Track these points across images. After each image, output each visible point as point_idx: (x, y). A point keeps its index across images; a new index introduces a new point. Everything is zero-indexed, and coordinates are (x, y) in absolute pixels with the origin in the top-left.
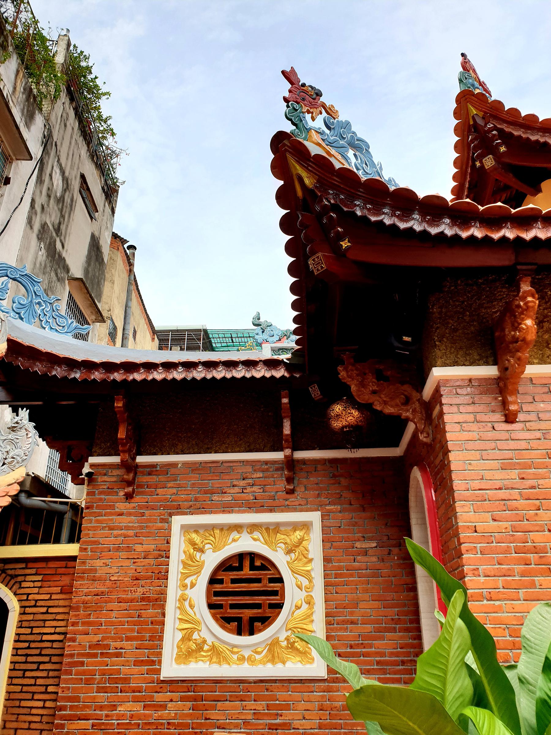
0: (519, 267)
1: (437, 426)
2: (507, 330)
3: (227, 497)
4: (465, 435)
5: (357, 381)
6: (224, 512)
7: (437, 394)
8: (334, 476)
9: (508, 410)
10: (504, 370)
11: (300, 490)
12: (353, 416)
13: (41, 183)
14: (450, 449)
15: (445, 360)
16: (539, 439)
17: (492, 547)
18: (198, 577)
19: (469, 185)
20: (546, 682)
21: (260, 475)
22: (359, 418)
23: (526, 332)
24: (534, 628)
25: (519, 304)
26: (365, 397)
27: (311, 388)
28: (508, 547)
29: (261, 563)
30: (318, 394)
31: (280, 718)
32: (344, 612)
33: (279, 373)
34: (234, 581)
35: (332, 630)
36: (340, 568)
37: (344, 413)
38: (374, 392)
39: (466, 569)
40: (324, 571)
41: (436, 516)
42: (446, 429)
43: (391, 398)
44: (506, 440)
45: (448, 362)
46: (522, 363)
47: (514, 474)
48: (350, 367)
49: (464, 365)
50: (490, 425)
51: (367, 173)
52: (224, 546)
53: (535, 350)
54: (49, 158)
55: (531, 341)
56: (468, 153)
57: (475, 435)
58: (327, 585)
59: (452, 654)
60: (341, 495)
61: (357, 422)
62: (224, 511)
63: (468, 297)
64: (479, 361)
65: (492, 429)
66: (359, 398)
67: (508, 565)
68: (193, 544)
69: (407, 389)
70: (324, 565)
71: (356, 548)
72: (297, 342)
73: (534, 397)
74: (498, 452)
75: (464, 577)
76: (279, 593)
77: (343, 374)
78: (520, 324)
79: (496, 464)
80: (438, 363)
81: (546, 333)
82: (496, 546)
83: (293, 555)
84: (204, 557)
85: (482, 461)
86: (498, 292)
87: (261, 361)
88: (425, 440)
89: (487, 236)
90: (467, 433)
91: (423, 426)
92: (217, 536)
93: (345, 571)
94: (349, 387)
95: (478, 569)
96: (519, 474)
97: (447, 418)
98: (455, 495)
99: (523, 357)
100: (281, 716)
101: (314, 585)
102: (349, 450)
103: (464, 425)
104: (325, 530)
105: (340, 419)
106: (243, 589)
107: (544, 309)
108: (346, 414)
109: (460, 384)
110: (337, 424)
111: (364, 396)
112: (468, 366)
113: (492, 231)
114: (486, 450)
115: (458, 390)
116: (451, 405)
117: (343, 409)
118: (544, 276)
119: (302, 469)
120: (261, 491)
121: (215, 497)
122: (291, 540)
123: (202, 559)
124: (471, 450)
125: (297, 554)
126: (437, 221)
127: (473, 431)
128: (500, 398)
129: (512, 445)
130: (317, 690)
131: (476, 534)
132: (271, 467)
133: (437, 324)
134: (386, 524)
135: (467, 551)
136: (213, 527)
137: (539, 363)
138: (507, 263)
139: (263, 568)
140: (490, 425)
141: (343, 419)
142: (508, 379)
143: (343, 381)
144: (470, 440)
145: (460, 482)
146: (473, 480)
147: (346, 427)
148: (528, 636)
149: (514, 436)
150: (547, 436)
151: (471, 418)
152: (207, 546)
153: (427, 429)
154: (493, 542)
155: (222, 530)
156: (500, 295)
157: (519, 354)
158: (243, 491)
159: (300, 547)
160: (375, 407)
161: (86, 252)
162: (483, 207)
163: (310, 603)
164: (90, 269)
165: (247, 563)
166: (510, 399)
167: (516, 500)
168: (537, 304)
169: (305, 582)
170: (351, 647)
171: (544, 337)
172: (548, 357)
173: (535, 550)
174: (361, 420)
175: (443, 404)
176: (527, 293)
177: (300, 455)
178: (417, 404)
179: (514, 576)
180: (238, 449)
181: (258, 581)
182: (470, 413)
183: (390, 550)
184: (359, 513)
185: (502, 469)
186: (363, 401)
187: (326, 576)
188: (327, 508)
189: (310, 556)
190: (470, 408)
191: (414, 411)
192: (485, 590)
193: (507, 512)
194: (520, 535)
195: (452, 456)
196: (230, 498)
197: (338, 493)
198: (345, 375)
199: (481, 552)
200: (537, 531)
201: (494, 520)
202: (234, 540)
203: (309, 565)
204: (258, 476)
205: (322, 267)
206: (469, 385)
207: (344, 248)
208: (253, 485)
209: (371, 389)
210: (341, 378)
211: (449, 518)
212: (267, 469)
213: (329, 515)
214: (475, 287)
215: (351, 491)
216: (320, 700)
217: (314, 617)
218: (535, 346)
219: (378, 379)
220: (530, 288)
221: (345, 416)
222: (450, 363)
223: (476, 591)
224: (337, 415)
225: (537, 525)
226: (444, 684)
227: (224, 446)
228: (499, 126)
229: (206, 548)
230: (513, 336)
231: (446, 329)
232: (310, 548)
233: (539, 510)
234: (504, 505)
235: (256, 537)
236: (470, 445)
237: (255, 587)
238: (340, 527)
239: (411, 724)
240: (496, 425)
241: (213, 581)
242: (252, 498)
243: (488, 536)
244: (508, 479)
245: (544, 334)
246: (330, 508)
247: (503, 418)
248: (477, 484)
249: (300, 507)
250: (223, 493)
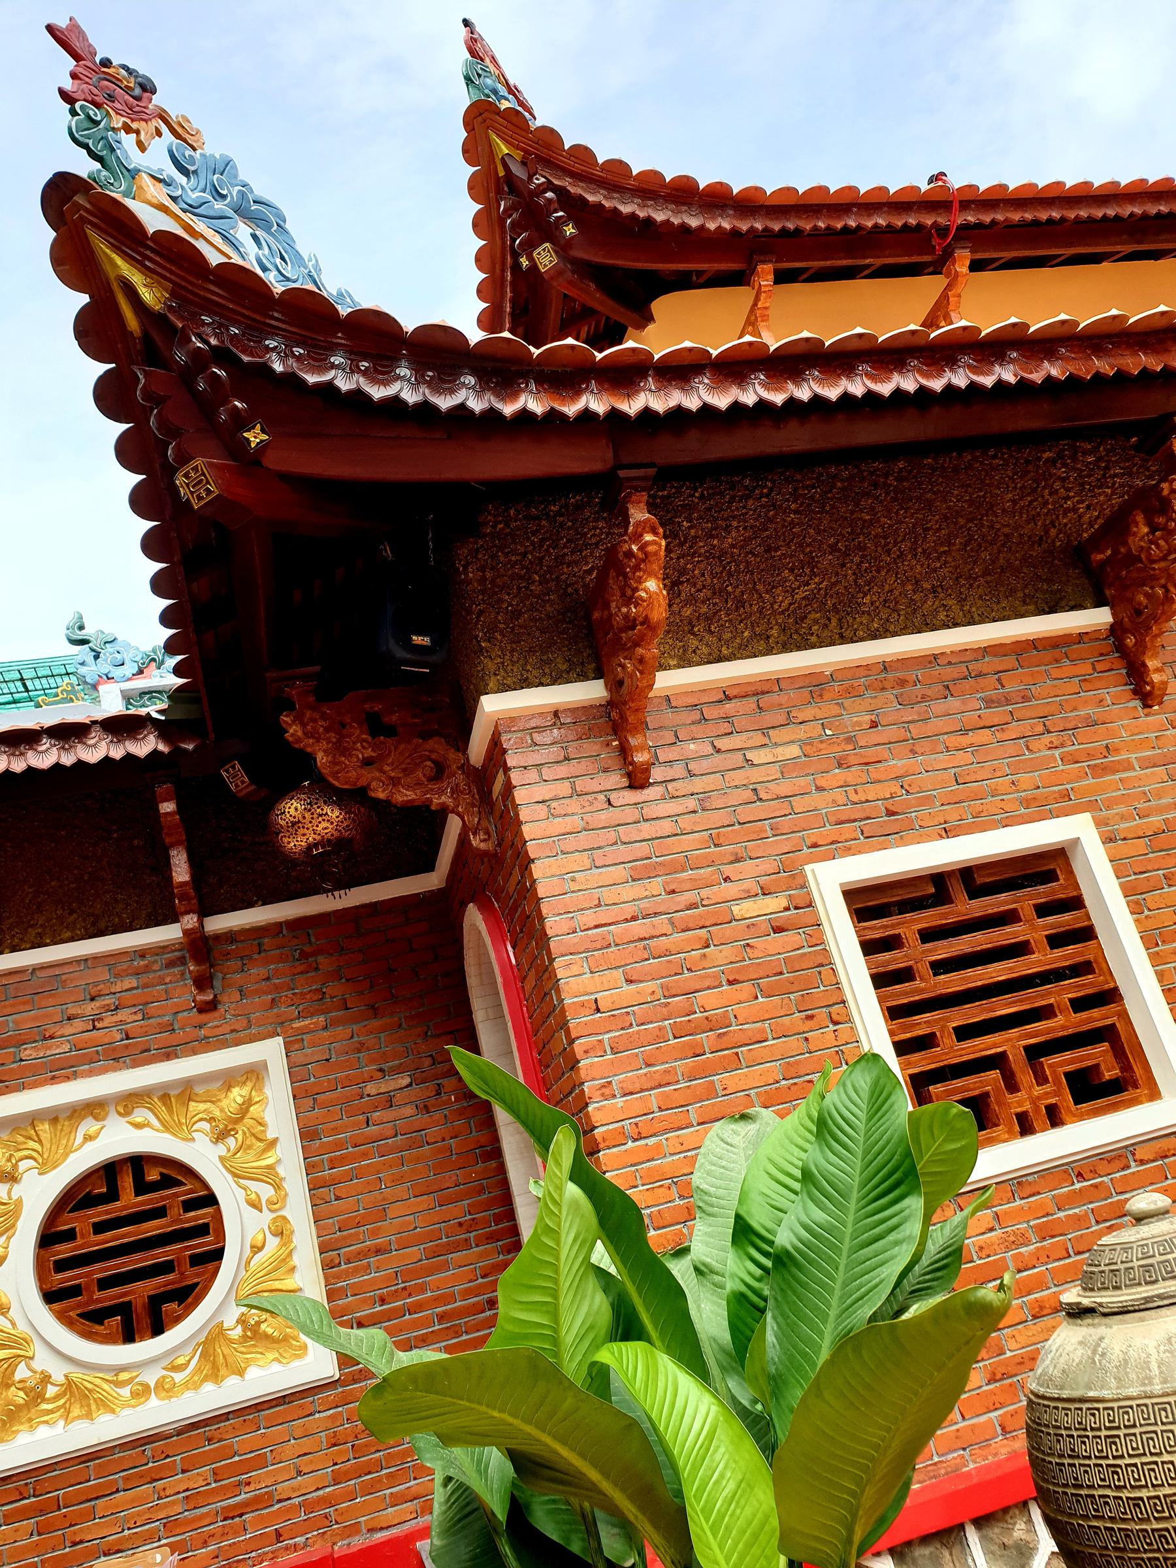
0: (622, 474)
1: (504, 815)
2: (613, 605)
3: (58, 1047)
4: (559, 825)
5: (327, 744)
6: (54, 1080)
7: (496, 750)
8: (304, 955)
9: (632, 763)
10: (615, 685)
11: (230, 1001)
12: (328, 821)
14: (532, 856)
15: (504, 678)
16: (694, 812)
17: (630, 1035)
18: (9, 1238)
19: (513, 307)
20: (740, 1258)
21: (131, 982)
22: (342, 822)
23: (648, 605)
24: (713, 1168)
25: (631, 549)
26: (350, 774)
27: (227, 771)
28: (660, 1029)
29: (161, 1174)
30: (243, 782)
31: (247, 1489)
32: (358, 1234)
33: (145, 746)
34: (99, 1228)
35: (338, 1277)
36: (339, 1145)
37: (308, 815)
38: (367, 762)
39: (589, 1088)
40: (305, 1159)
41: (522, 996)
42: (521, 818)
43: (404, 770)
44: (635, 823)
45: (509, 681)
46: (649, 669)
47: (656, 885)
48: (308, 714)
49: (541, 684)
50: (601, 797)
51: (288, 279)
52: (66, 1155)
53: (671, 642)
55: (658, 623)
56: (503, 239)
57: (576, 822)
58: (314, 1186)
59: (563, 1257)
60: (324, 993)
61: (340, 831)
62: (53, 1078)
63: (533, 543)
64: (568, 673)
65: (606, 806)
66: (337, 779)
67: (663, 1063)
69: (437, 746)
70: (303, 1147)
71: (369, 1095)
72: (178, 671)
73: (676, 732)
74: (622, 847)
75: (587, 1105)
76: (214, 1228)
77: (294, 731)
78: (636, 590)
79: (620, 872)
80: (491, 685)
81: (686, 605)
82: (638, 1032)
83: (231, 1141)
84: (17, 1190)
85: (595, 871)
86: (590, 530)
87: (94, 722)
88: (483, 846)
89: (552, 409)
90: (560, 819)
91: (476, 819)
92: (45, 1136)
93: (351, 1149)
94: (311, 758)
95: (610, 1083)
96: (665, 884)
97: (520, 795)
98: (552, 944)
99: (648, 655)
100: (249, 1484)
101: (286, 1195)
102: (330, 894)
103: (554, 804)
104: (296, 1072)
105: (301, 831)
106: (126, 1240)
107: (678, 558)
108: (312, 818)
109: (538, 724)
110: (295, 843)
111: (348, 772)
112: (548, 685)
113: (563, 401)
114: (599, 848)
115: (535, 735)
116: (525, 768)
117: (305, 809)
118: (673, 491)
119: (228, 954)
120: (140, 1016)
121: (28, 1052)
122: (222, 1110)
123: (15, 1197)
124: (572, 853)
125: (240, 1136)
126: (449, 382)
127: (573, 814)
128: (615, 743)
129: (647, 829)
130: (321, 1408)
131: (599, 1015)
132: (156, 961)
133: (479, 605)
134: (426, 1033)
135: (586, 1052)
136: (32, 1119)
137: (679, 666)
138: (597, 466)
139: (167, 1182)
140: (601, 797)
141: (308, 829)
142: (625, 703)
143: (297, 746)
144: (568, 833)
145: (557, 918)
146: (582, 910)
147: (316, 845)
148: (704, 1186)
149: (649, 812)
150: (707, 805)
151: (564, 788)
152: (23, 1165)
153: (484, 823)
154: (631, 1024)
155: (55, 1120)
156: (594, 535)
157: (640, 651)
158: (94, 1027)
159: (246, 1121)
160: (373, 795)
162: (538, 348)
163: (282, 1233)
165: (127, 1182)
166: (633, 741)
167: (665, 935)
168: (663, 548)
169: (266, 1192)
170: (383, 1301)
171: (683, 613)
172: (694, 652)
173: (710, 1024)
174: (347, 826)
175: (510, 769)
176: (644, 526)
177: (219, 923)
178: (460, 778)
179: (677, 1082)
180: (69, 934)
181: (160, 1213)
182: (563, 779)
183: (438, 1085)
184: (366, 1023)
185: (634, 880)
186: (346, 783)
187: (310, 1169)
188: (296, 1025)
189: (270, 1135)
190: (563, 770)
191: (455, 791)
192: (628, 1122)
193: (651, 961)
194: (680, 1002)
195: (537, 870)
196: (66, 1047)
198: (300, 733)
199: (612, 1048)
200: (709, 988)
201: (630, 981)
202: (88, 1138)
203: (270, 1154)
204: (127, 985)
205: (209, 492)
206: (555, 724)
207: (253, 445)
208: (117, 1008)
209: (360, 756)
210: (290, 739)
211: (545, 994)
212: (147, 966)
213: (303, 1040)
214: (544, 522)
215: (344, 980)
216: (330, 1425)
217: (296, 1260)
218: (668, 632)
219: (374, 733)
220: (647, 515)
221: (311, 822)
222: (514, 683)
223: (611, 1127)
224: (294, 824)
225: (708, 976)
226: (555, 1316)
227: (32, 932)
228: (556, 182)
229: (21, 1170)
230: (626, 617)
231: (498, 613)
232: (268, 1117)
233: (708, 946)
234: (645, 948)
235: (139, 1120)
236: (570, 843)
237: (153, 1228)
238: (327, 1060)
239: (496, 1414)
240: (613, 796)
241: (48, 1238)
242: (119, 1037)
243: (622, 1014)
244: (646, 897)
245: (682, 607)
246: (302, 1023)
247: (625, 782)
248: (589, 918)
249: (234, 1035)
250: (45, 1039)
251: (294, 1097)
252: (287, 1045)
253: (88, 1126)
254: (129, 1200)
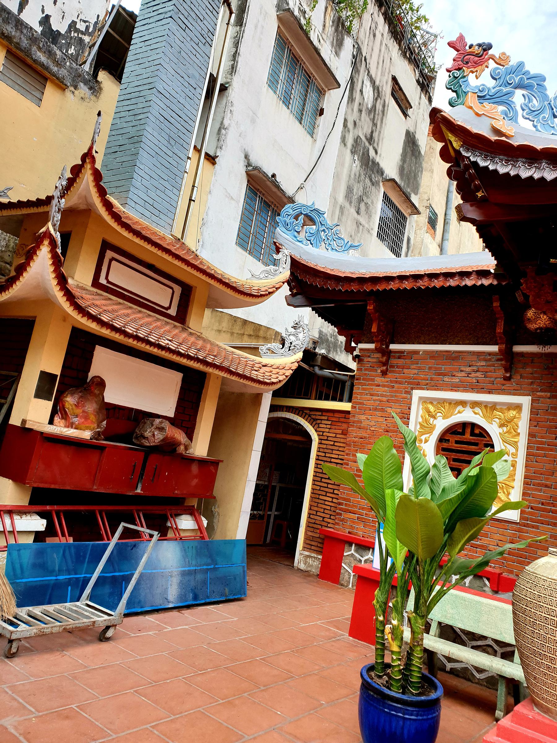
3: (455, 379)
6: (452, 390)
11: (516, 378)
13: (352, 102)
18: (430, 435)
21: (483, 363)
27: (517, 293)
29: (480, 432)
31: (480, 541)
32: (539, 477)
33: (486, 282)
34: (457, 442)
35: (529, 489)
36: (542, 443)
40: (528, 443)
52: (451, 416)
54: (359, 75)
62: (452, 389)
68: (429, 412)
70: (528, 439)
83: (505, 429)
84: (435, 422)
87: (473, 271)
92: (447, 408)
100: (481, 540)
104: (534, 411)
106: (464, 449)
110: (532, 326)
119: (520, 361)
120: (483, 376)
121: (446, 379)
122: (505, 416)
123: (434, 423)
125: (508, 428)
130: (510, 529)
132: (493, 358)
152: (439, 414)
155: (450, 403)
158: (468, 376)
159: (512, 423)
161: (400, 151)
164: (405, 166)
165: (468, 431)
170: (543, 504)
180: (468, 342)
188: (538, 394)
189: (519, 431)
196: (458, 380)
197: (550, 383)
202: (459, 412)
203: (517, 437)
204: (482, 364)
208: (477, 371)
212: (490, 359)
227: (456, 339)
229: (438, 416)
235: (476, 411)
238: (547, 410)
242: (475, 381)
246: (541, 394)
249: (515, 391)
250: (452, 376)
251: (530, 420)
252: (532, 400)
253: (460, 408)
254: (468, 436)
